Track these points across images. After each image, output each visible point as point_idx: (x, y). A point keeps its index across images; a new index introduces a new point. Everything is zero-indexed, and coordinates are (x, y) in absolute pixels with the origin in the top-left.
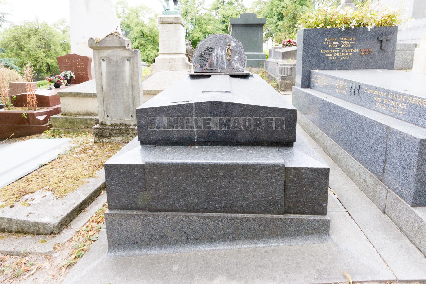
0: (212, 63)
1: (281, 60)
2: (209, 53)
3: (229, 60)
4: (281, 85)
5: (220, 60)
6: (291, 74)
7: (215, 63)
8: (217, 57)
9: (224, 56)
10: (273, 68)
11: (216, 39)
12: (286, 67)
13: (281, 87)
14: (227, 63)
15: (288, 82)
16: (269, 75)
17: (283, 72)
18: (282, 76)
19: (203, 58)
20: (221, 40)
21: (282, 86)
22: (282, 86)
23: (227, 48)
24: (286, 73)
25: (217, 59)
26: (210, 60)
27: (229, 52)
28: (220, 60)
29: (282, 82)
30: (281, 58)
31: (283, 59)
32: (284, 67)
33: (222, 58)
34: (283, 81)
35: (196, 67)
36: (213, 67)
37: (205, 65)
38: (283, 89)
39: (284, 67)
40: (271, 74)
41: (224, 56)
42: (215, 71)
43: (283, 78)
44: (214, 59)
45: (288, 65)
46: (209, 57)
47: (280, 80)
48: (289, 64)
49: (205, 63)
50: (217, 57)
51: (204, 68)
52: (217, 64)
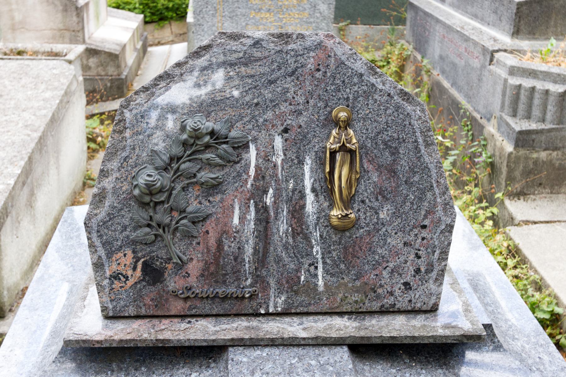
0: (229, 247)
1: (506, 40)
2: (205, 175)
3: (340, 230)
4: (510, 171)
5: (282, 227)
6: (560, 122)
7: (249, 250)
8: (262, 210)
9: (310, 198)
10: (461, 63)
11: (256, 69)
12: (540, 85)
13: (510, 179)
14: (326, 252)
15: (543, 155)
16: (438, 85)
17: (522, 107)
18: (521, 133)
19: (161, 216)
20: (289, 84)
21: (517, 174)
22: (517, 174)
23: (332, 144)
24: (536, 112)
25: (264, 221)
26: (210, 225)
27: (342, 173)
28: (282, 227)
29: (518, 158)
30: (509, 27)
31: (516, 33)
32: (527, 83)
33: (297, 212)
34: (522, 152)
35: (115, 277)
36: (237, 274)
37: (181, 265)
38: (518, 186)
39: (527, 83)
40: (446, 84)
41: (310, 198)
42: (247, 306)
43: (523, 139)
44: (241, 219)
45: (547, 76)
46: (206, 207)
47: (509, 148)
48: (555, 70)
49: (178, 248)
50: (262, 210)
51: (173, 283)
52: (262, 257)
